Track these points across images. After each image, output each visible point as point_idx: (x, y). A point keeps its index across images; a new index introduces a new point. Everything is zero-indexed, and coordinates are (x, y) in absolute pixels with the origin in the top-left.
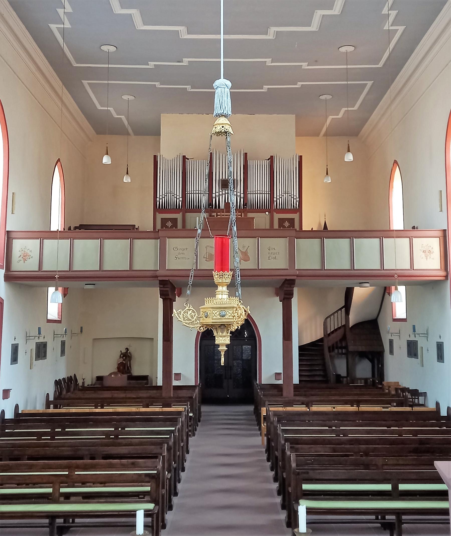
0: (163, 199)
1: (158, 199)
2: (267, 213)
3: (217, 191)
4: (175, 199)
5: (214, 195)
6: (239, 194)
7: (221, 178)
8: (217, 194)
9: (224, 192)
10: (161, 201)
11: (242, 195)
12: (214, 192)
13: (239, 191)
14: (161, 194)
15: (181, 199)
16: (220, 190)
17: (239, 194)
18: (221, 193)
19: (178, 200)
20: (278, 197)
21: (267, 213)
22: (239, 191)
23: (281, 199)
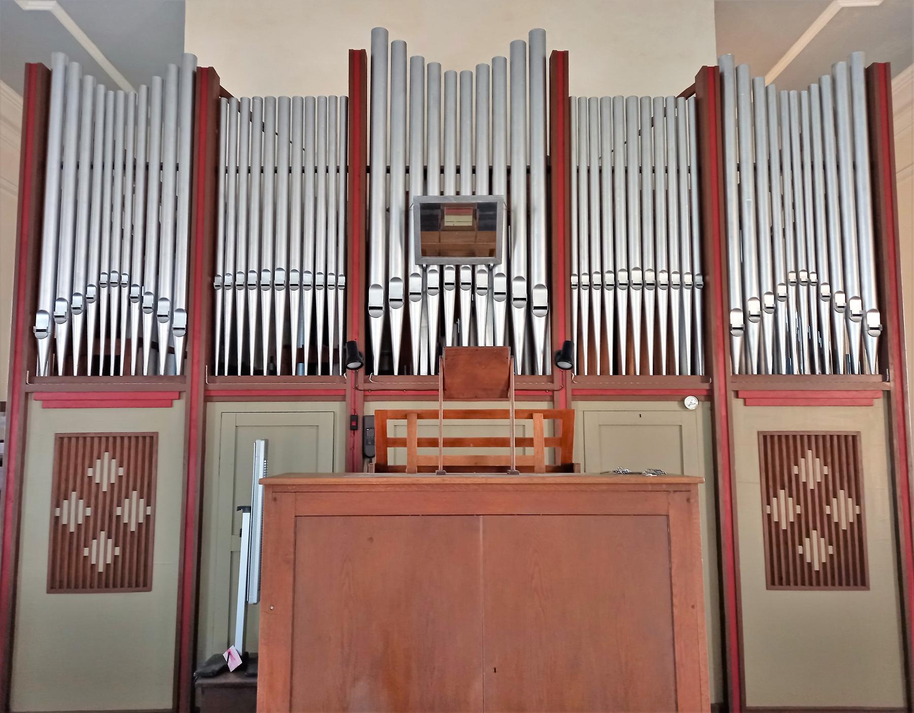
0: (78, 320)
1: (42, 321)
2: (691, 402)
3: (397, 270)
4: (148, 318)
5: (376, 298)
6: (519, 290)
7: (416, 191)
8: (396, 290)
9: (433, 280)
10: (62, 329)
11: (540, 297)
12: (377, 276)
13: (519, 269)
14: (64, 292)
15: (181, 320)
16: (414, 268)
17: (519, 290)
18: (415, 284)
19: (163, 329)
20: (753, 307)
21: (691, 402)
22: (519, 269)
23: (768, 318)
